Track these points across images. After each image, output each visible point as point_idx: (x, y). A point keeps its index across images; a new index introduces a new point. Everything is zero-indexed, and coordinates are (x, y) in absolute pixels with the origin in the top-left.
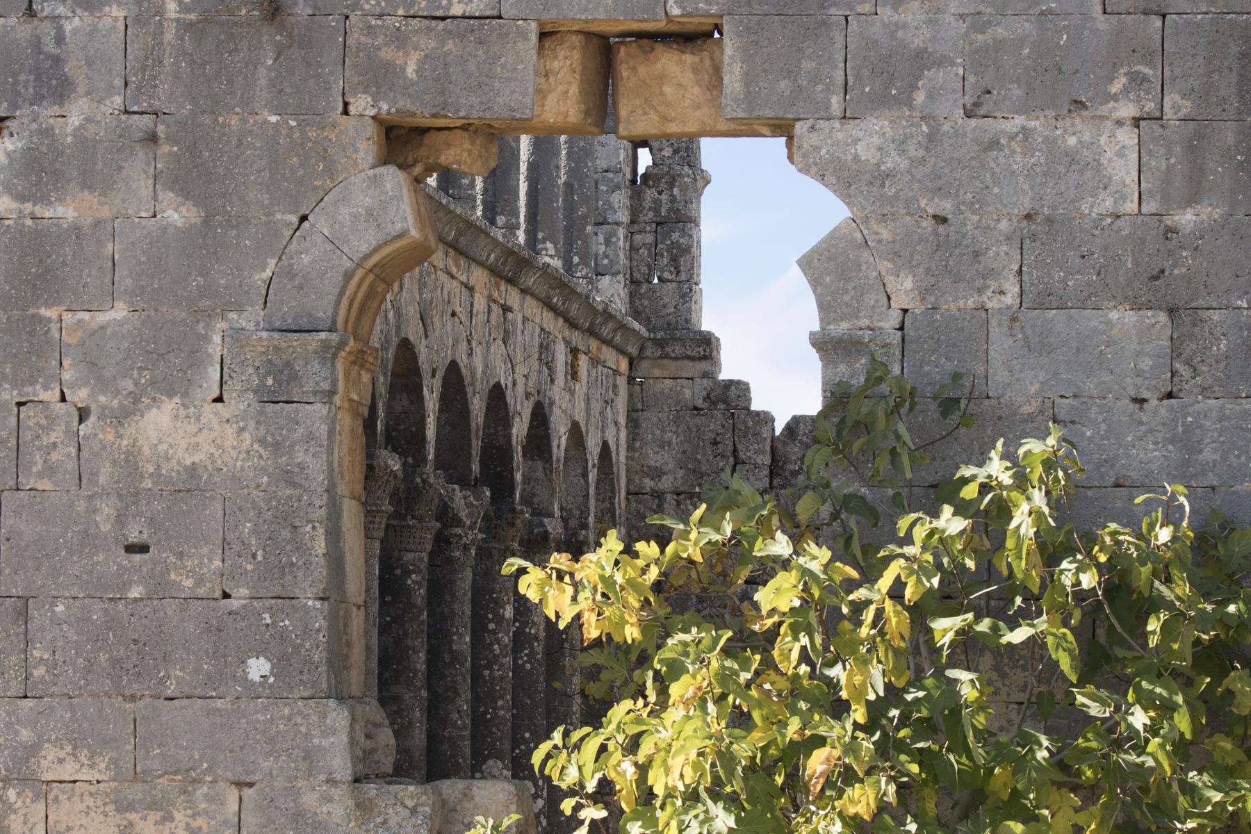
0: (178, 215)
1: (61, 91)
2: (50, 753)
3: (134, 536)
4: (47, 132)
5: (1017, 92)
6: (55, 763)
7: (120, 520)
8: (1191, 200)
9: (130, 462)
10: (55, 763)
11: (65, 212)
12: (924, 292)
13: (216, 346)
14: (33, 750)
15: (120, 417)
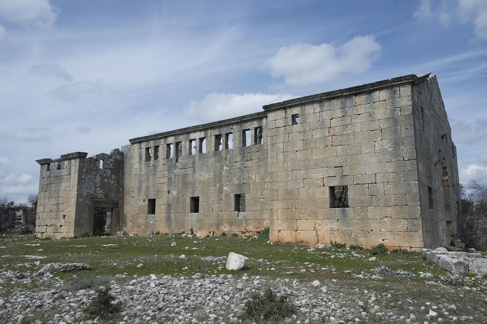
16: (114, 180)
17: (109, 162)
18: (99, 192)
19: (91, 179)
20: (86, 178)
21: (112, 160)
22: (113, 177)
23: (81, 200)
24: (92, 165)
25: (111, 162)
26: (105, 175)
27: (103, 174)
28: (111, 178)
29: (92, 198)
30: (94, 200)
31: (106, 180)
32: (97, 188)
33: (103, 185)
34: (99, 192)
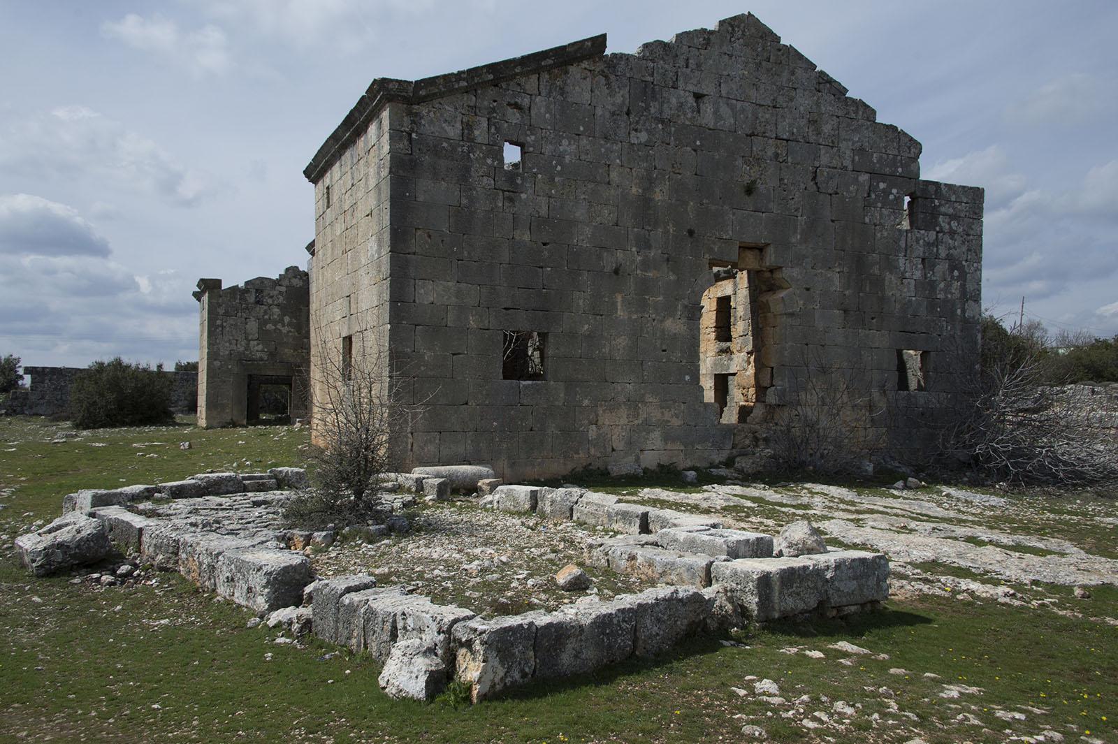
0: (672, 277)
1: (649, 247)
2: (647, 396)
3: (664, 348)
4: (647, 256)
5: (820, 264)
6: (649, 398)
7: (661, 345)
8: (848, 289)
9: (663, 331)
10: (649, 398)
11: (650, 274)
12: (804, 304)
13: (679, 307)
14: (644, 395)
15: (662, 321)
16: (289, 324)
17: (275, 293)
18: (256, 348)
19: (236, 325)
20: (225, 324)
21: (283, 289)
22: (287, 319)
23: (217, 363)
24: (238, 301)
25: (281, 293)
26: (266, 317)
27: (263, 316)
28: (282, 321)
29: (241, 360)
30: (243, 360)
31: (270, 327)
32: (251, 342)
33: (263, 335)
34: (256, 348)
